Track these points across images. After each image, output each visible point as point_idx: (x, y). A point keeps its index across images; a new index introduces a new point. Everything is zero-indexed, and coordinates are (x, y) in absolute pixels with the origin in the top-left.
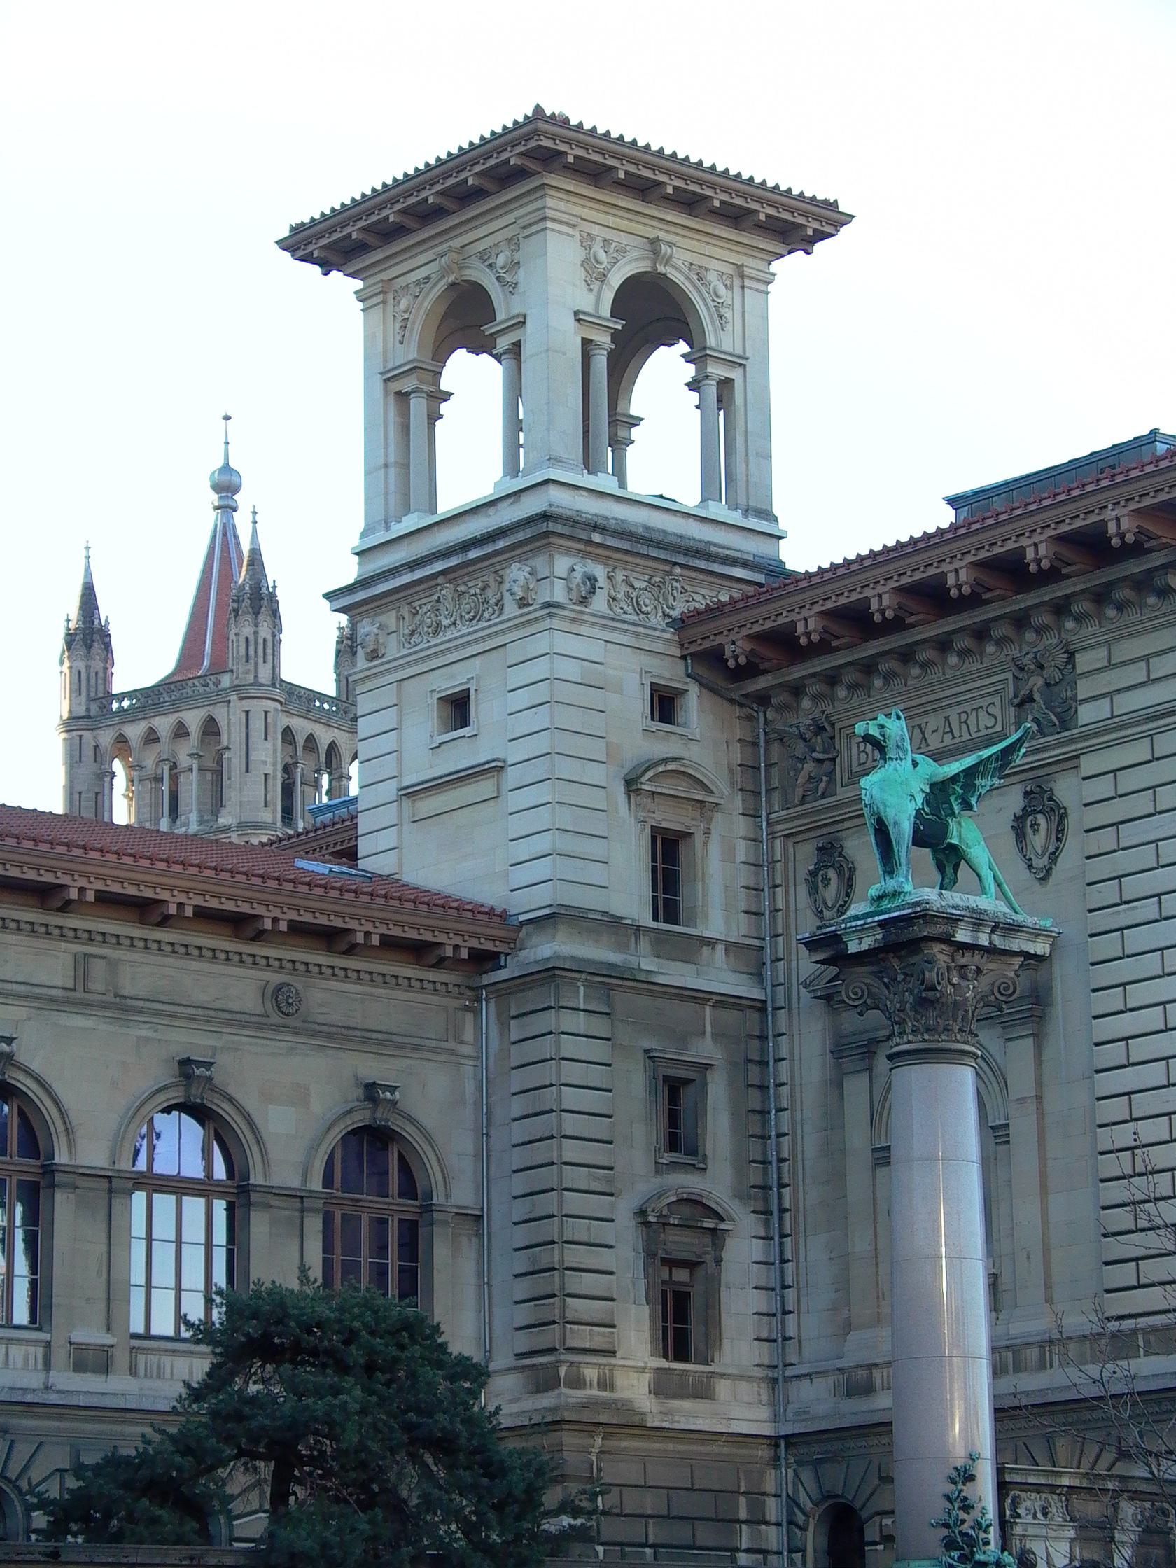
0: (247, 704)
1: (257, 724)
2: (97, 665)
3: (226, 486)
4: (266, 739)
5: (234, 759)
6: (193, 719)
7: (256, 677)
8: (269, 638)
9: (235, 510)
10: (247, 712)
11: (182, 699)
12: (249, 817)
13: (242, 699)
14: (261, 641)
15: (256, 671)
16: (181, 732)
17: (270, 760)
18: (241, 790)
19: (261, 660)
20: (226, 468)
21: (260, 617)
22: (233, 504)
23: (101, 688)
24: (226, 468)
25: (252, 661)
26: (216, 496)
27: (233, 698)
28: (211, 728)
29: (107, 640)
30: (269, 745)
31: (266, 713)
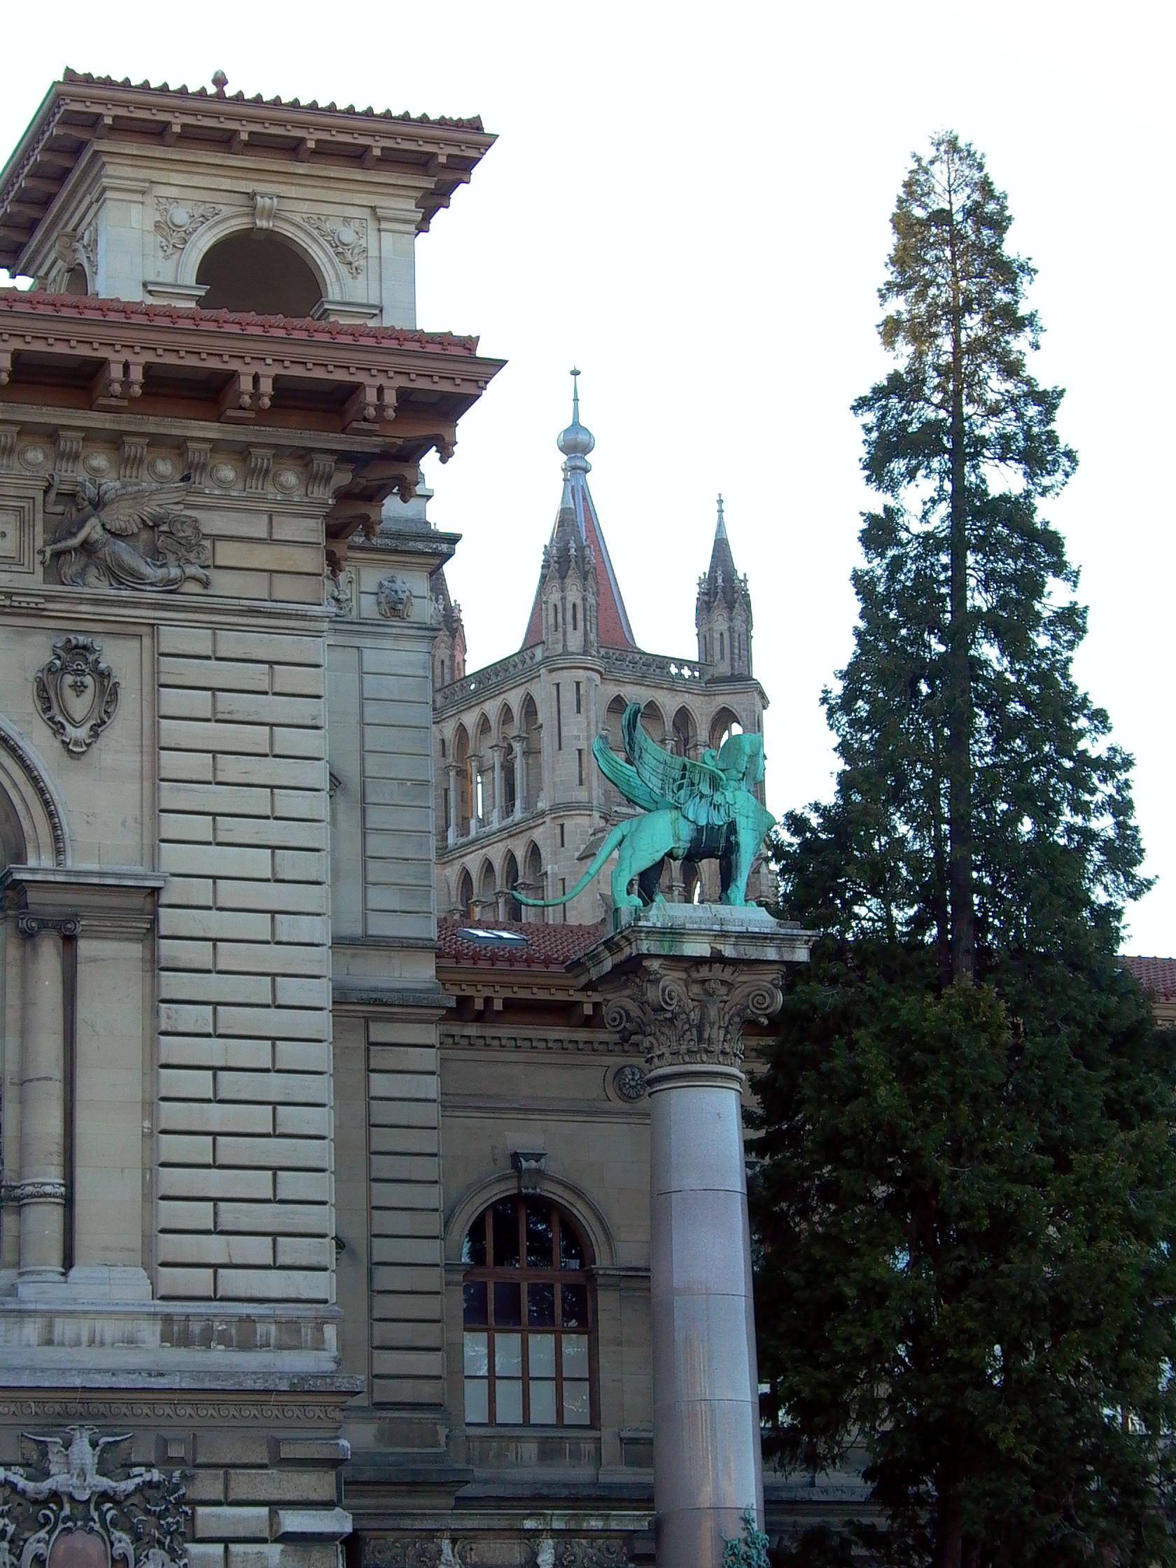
0: (557, 677)
1: (569, 696)
2: (443, 653)
3: (576, 446)
4: (579, 711)
5: (546, 739)
6: (514, 699)
7: (565, 645)
8: (579, 602)
9: (586, 471)
10: (558, 685)
11: (504, 681)
12: (561, 798)
13: (551, 671)
14: (569, 606)
15: (565, 640)
16: (507, 710)
17: (583, 734)
18: (554, 770)
19: (570, 627)
20: (576, 426)
21: (568, 581)
22: (584, 465)
23: (447, 677)
24: (576, 426)
25: (560, 629)
26: (565, 458)
27: (543, 671)
28: (530, 706)
29: (455, 625)
30: (581, 718)
31: (578, 684)
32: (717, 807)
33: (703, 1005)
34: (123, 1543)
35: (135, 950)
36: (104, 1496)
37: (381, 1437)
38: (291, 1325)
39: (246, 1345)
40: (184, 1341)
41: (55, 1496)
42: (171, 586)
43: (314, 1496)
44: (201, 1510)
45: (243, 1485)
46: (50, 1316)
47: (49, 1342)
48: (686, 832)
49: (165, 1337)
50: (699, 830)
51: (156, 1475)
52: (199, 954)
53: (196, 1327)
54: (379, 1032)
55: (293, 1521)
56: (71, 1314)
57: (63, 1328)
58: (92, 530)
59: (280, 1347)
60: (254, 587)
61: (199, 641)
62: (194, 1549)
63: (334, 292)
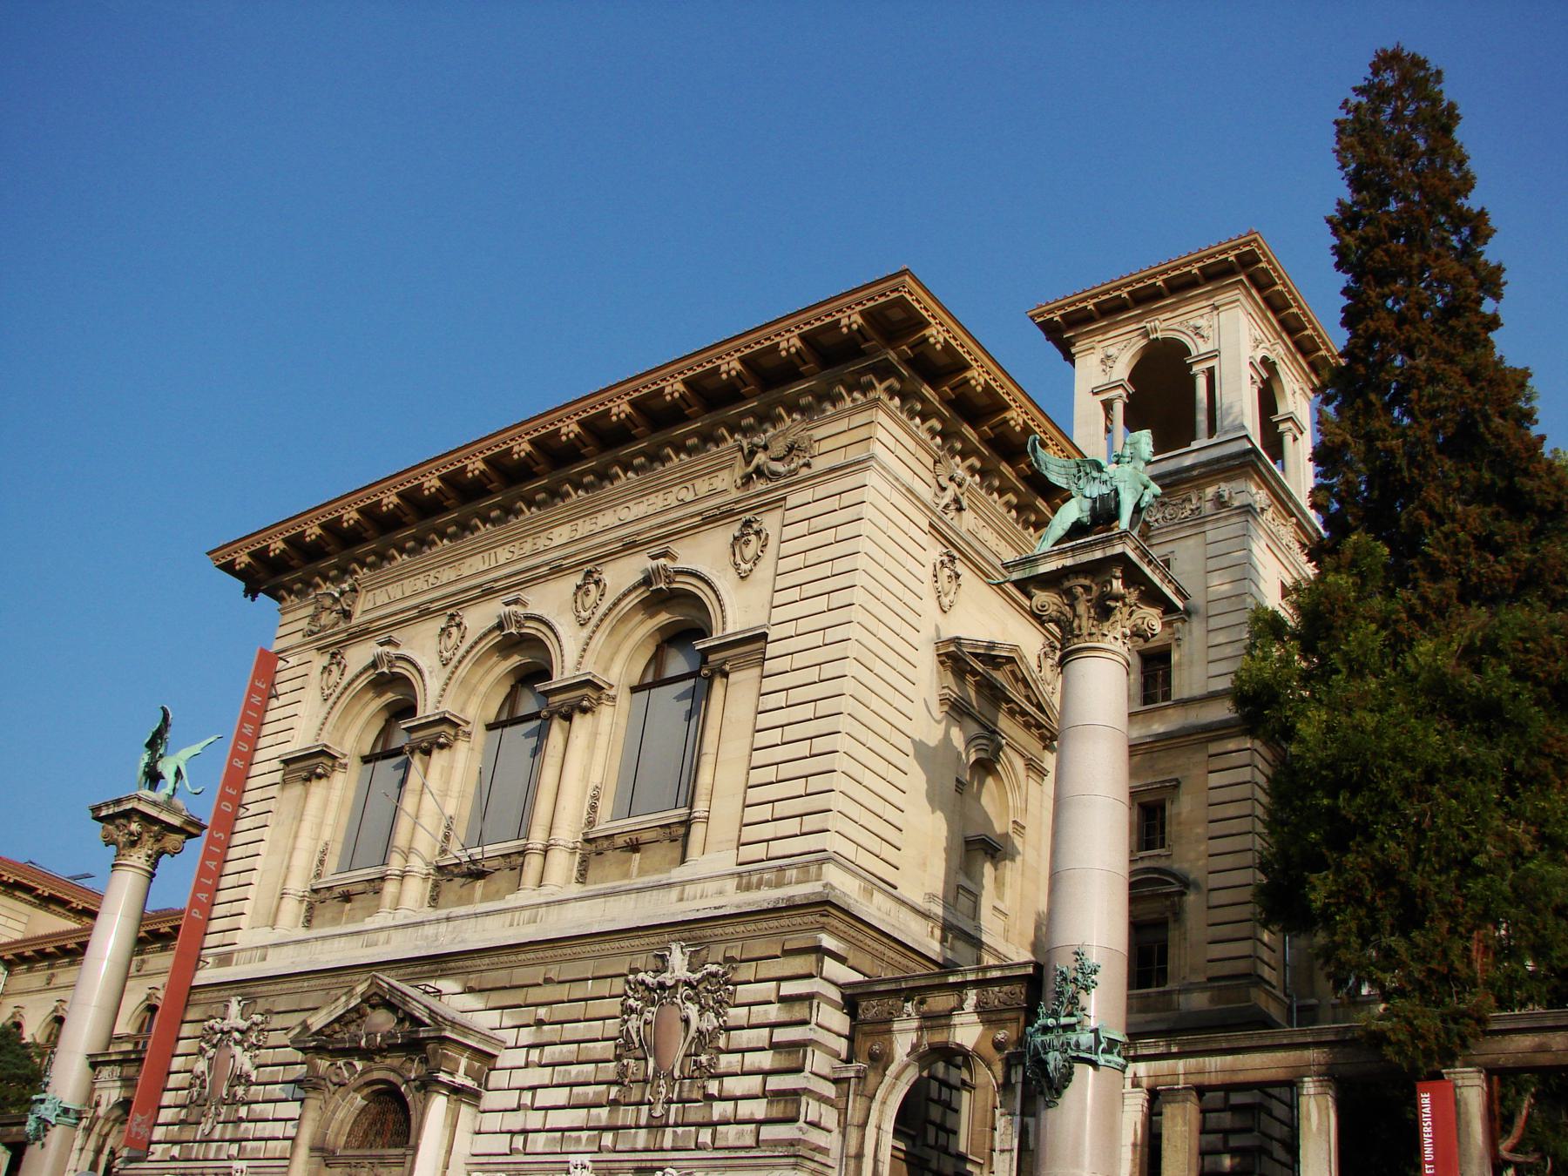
32: (1105, 482)
33: (1072, 606)
34: (692, 1010)
35: (756, 671)
36: (688, 983)
37: (1212, 1000)
38: (806, 865)
39: (779, 884)
40: (748, 888)
41: (662, 986)
42: (794, 472)
43: (801, 972)
44: (739, 987)
45: (767, 969)
46: (683, 883)
47: (681, 900)
48: (1087, 504)
49: (739, 887)
50: (1094, 500)
51: (714, 968)
52: (783, 664)
53: (755, 879)
54: (1214, 748)
55: (788, 989)
56: (692, 881)
57: (689, 889)
58: (760, 458)
59: (798, 883)
60: (837, 459)
61: (807, 495)
62: (731, 1011)
63: (1194, 353)
